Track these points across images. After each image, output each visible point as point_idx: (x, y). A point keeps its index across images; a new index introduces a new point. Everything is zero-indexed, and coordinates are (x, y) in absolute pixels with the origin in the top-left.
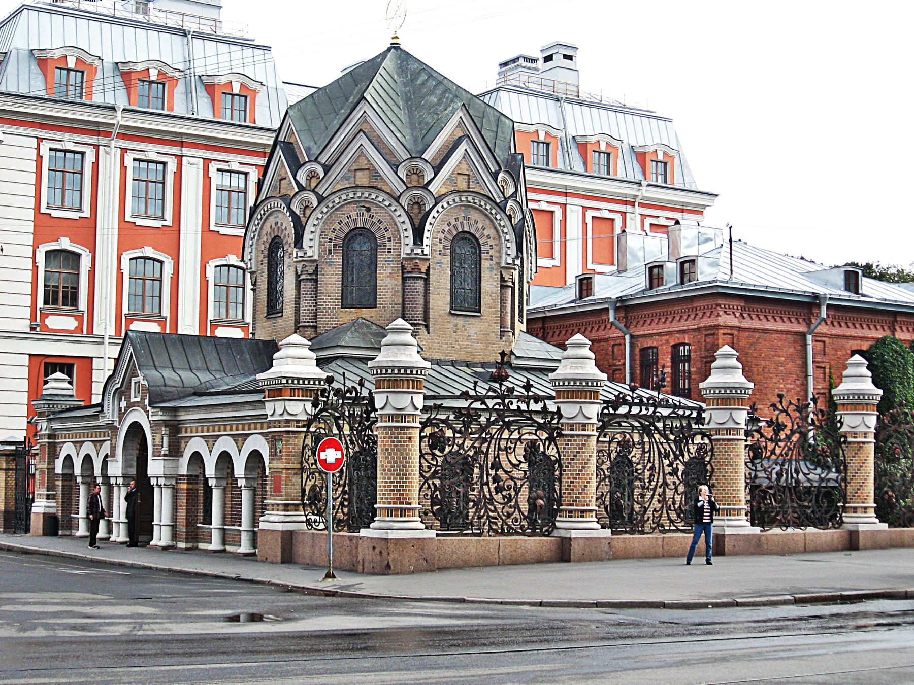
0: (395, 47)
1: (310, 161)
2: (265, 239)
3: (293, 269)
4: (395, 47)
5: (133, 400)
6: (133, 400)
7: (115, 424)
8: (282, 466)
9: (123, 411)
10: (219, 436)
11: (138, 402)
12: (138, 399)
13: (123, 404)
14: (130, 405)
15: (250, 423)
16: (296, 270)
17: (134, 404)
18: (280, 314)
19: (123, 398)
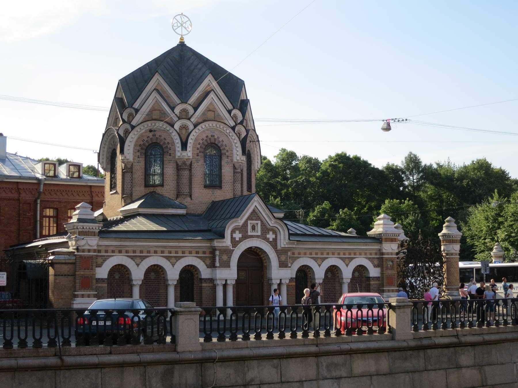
0: (182, 45)
1: (234, 108)
2: (201, 142)
3: (232, 165)
4: (182, 45)
5: (250, 233)
6: (250, 233)
7: (230, 247)
8: (394, 272)
9: (237, 239)
10: (327, 258)
11: (259, 236)
12: (259, 233)
13: (238, 236)
14: (245, 237)
15: (356, 253)
16: (234, 166)
17: (252, 237)
18: (219, 188)
19: (237, 232)
